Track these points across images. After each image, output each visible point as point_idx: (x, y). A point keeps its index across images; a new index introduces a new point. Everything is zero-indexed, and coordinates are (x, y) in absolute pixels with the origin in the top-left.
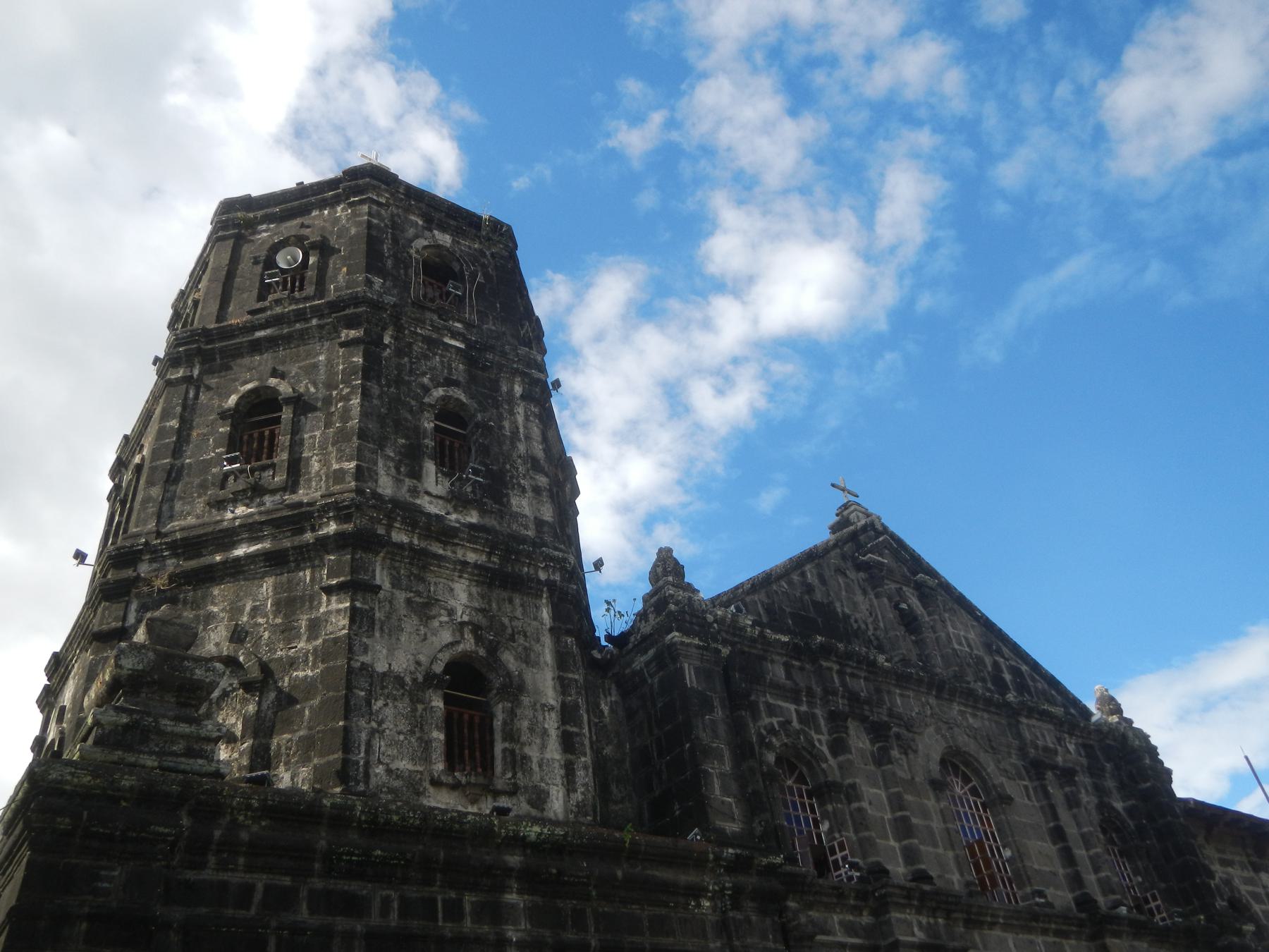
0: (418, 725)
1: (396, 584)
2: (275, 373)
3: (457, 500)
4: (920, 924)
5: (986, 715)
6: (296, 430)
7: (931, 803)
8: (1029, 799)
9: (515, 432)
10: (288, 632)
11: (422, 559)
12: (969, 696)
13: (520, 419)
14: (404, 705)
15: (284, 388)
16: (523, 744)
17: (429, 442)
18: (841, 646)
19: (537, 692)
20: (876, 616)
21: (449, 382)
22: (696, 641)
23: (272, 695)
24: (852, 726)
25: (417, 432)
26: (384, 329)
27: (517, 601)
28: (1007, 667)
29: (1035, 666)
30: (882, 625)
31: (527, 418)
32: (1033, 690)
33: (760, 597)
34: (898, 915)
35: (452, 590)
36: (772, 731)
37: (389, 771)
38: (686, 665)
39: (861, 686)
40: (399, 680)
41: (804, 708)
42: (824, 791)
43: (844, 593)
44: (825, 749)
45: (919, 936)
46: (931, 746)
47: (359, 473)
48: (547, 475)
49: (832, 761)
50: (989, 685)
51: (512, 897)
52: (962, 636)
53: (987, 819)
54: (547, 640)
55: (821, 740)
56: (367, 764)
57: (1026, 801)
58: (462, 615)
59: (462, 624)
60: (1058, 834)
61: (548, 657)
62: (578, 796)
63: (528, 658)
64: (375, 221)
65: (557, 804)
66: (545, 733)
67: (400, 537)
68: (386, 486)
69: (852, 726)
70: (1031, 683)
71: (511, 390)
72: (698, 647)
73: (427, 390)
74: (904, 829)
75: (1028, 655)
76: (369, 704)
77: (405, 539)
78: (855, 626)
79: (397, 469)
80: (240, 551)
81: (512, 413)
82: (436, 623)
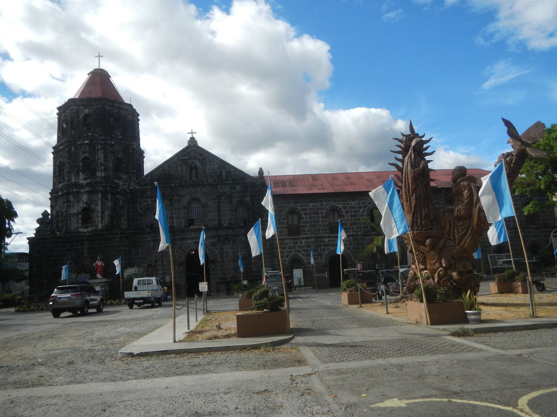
0: (78, 220)
1: (74, 198)
2: (62, 157)
3: (85, 179)
5: (209, 187)
6: (64, 170)
8: (215, 204)
9: (98, 158)
11: (78, 193)
13: (100, 154)
15: (62, 161)
21: (86, 152)
22: (122, 197)
23: (63, 217)
25: (79, 166)
27: (95, 195)
30: (184, 173)
31: (101, 154)
35: (83, 197)
36: (144, 206)
37: (74, 227)
38: (121, 201)
40: (74, 214)
46: (186, 200)
47: (69, 180)
48: (103, 166)
50: (216, 178)
51: (86, 243)
54: (100, 200)
57: (214, 204)
58: (85, 201)
59: (84, 203)
60: (219, 211)
61: (100, 203)
62: (103, 225)
63: (96, 205)
64: (72, 115)
65: (100, 226)
66: (98, 216)
67: (75, 190)
68: (73, 180)
70: (232, 173)
71: (98, 147)
73: (80, 156)
76: (70, 219)
77: (75, 190)
78: (175, 176)
80: (60, 193)
81: (98, 153)
82: (80, 203)
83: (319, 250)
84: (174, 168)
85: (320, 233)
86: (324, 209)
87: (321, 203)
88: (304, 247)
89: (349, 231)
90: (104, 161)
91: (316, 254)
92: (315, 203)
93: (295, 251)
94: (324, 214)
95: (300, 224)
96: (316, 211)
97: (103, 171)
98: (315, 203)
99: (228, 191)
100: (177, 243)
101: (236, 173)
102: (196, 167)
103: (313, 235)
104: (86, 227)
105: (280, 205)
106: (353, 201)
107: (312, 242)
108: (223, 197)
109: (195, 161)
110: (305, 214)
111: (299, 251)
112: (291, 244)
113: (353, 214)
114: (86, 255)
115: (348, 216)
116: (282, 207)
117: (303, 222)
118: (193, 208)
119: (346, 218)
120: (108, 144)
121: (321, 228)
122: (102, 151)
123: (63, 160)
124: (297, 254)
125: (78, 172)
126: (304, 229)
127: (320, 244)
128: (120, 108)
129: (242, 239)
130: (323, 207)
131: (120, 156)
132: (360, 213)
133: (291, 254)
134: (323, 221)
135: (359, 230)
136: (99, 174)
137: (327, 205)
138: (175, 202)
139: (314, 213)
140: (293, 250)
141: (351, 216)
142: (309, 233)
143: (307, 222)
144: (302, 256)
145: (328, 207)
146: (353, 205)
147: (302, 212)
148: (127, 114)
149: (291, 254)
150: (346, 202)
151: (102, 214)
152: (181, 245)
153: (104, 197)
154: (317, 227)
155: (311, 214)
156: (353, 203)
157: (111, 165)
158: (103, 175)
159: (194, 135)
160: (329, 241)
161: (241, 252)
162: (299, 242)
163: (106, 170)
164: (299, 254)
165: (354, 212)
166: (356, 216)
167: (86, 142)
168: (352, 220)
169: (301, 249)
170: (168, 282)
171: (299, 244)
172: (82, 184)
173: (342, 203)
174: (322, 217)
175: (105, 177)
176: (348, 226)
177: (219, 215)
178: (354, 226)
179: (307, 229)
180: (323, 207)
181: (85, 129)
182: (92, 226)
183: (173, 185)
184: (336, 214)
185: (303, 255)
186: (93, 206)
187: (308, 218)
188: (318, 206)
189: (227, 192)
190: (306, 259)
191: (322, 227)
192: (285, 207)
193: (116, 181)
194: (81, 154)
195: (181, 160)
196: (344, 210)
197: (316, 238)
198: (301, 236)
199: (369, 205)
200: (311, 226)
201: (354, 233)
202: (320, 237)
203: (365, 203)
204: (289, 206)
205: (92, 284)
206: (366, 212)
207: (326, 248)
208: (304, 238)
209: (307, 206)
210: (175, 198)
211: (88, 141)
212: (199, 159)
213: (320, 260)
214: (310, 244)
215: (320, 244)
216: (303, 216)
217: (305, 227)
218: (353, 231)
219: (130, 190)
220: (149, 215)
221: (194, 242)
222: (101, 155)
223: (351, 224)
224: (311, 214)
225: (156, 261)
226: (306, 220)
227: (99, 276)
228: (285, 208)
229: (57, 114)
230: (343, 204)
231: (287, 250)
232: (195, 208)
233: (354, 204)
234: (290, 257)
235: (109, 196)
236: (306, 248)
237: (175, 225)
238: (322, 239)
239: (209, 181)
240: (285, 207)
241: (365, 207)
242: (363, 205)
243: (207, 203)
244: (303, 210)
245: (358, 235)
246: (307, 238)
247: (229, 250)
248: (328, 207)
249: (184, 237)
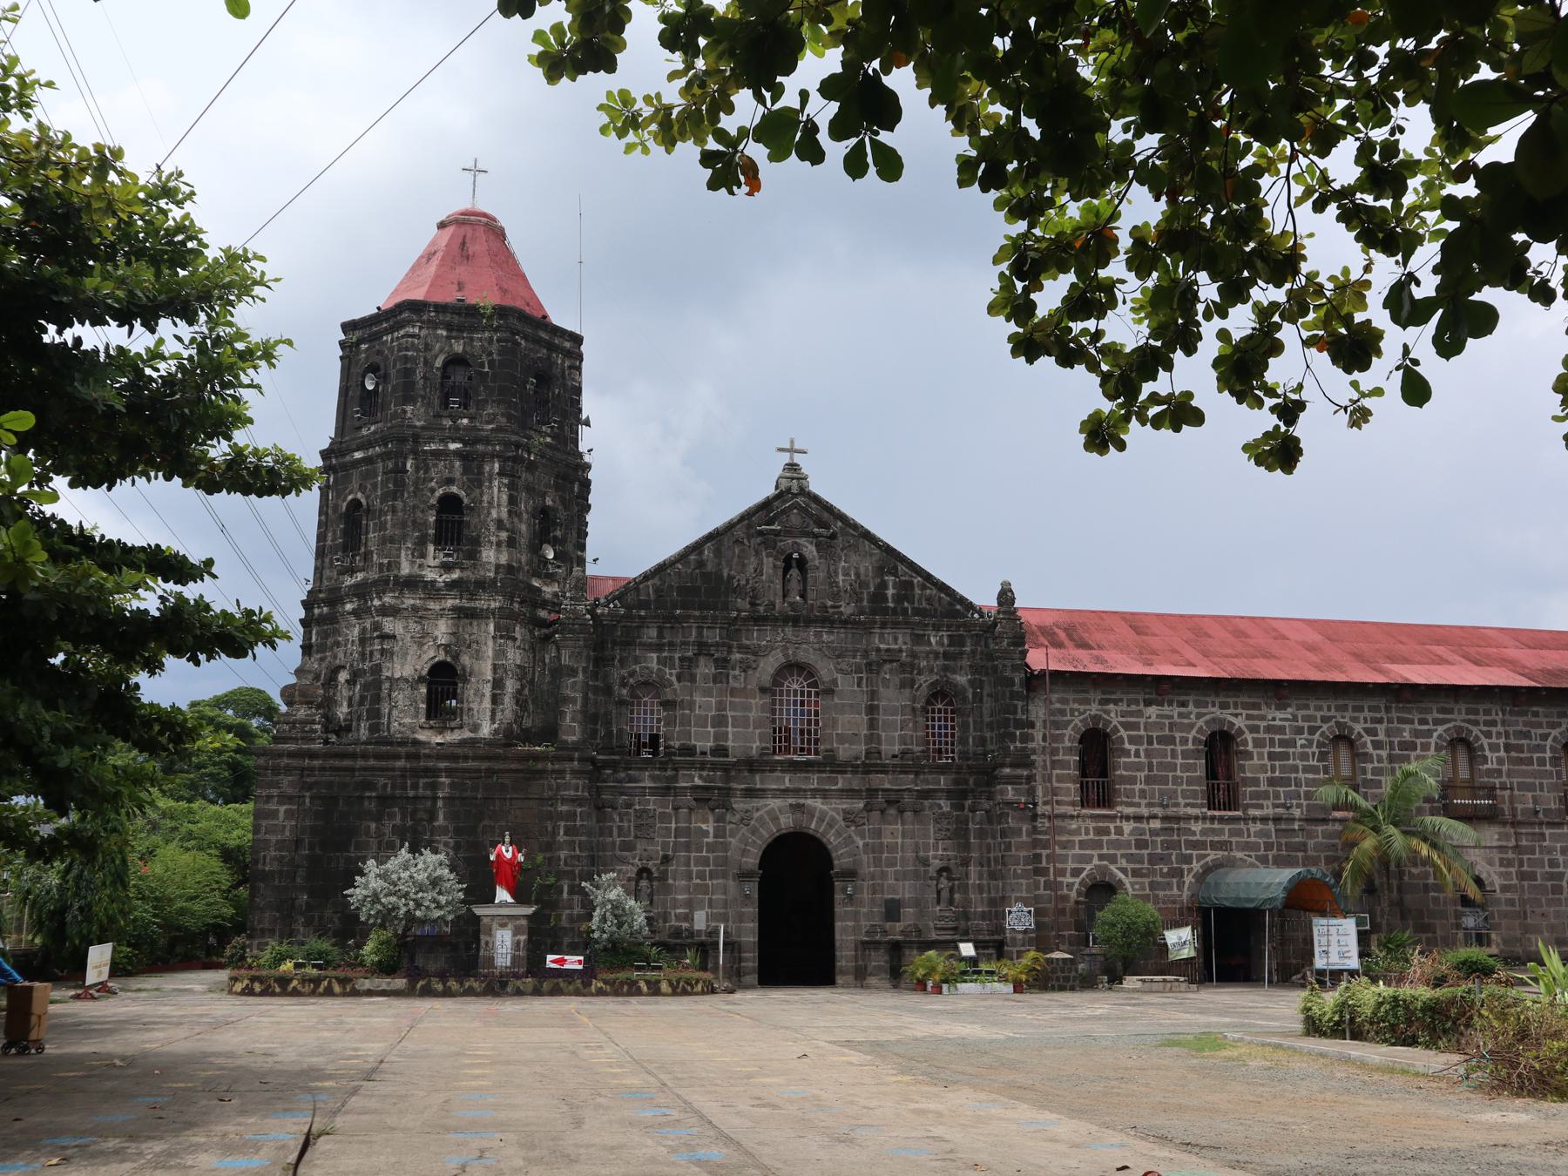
2: (362, 488)
3: (447, 568)
4: (701, 777)
7: (757, 701)
8: (859, 685)
10: (363, 654)
12: (827, 620)
14: (408, 692)
15: (363, 501)
16: (469, 703)
17: (432, 532)
18: (697, 613)
19: (481, 673)
20: (761, 572)
21: (450, 481)
24: (702, 661)
25: (426, 522)
26: (406, 458)
27: (475, 623)
28: (895, 583)
29: (928, 577)
31: (499, 491)
33: (656, 581)
36: (632, 674)
39: (713, 636)
40: (406, 680)
41: (665, 654)
42: (668, 705)
43: (736, 559)
44: (674, 679)
45: (698, 782)
46: (768, 666)
49: (676, 685)
52: (850, 568)
53: (816, 702)
54: (490, 643)
55: (671, 674)
56: (389, 723)
57: (856, 688)
60: (872, 710)
61: (490, 653)
62: (496, 726)
63: (478, 656)
66: (483, 695)
68: (405, 569)
69: (702, 661)
70: (918, 591)
73: (433, 491)
74: (720, 721)
76: (390, 695)
79: (413, 554)
81: (490, 487)
83: (1173, 858)
84: (736, 559)
85: (1176, 805)
86: (1191, 726)
87: (1182, 710)
88: (1128, 845)
89: (1265, 803)
90: (510, 512)
91: (1165, 870)
92: (1166, 707)
93: (1101, 857)
94: (1190, 746)
95: (1118, 773)
96: (1167, 732)
97: (504, 548)
98: (1166, 707)
99: (904, 647)
100: (735, 806)
102: (802, 563)
103: (1158, 811)
104: (441, 730)
105: (1058, 706)
106: (1279, 708)
107: (1153, 832)
108: (887, 667)
109: (802, 541)
110: (1132, 740)
111: (1113, 859)
112: (1087, 833)
113: (1278, 750)
114: (441, 820)
115: (1261, 756)
116: (1062, 712)
117: (1128, 767)
118: (788, 695)
119: (1256, 761)
120: (522, 459)
121: (1179, 788)
122: (506, 481)
123: (367, 498)
124: (1106, 866)
125: (421, 543)
126: (1128, 787)
127: (1175, 837)
128: (552, 347)
129: (941, 808)
130: (1186, 721)
131: (549, 502)
132: (1299, 750)
133: (1088, 867)
134: (1186, 768)
135: (1294, 802)
136: (489, 555)
137: (1199, 716)
138: (733, 669)
139: (1161, 740)
140: (1095, 853)
141: (1272, 756)
142: (1144, 802)
143: (1139, 767)
144: (1121, 875)
145: (1201, 722)
146: (1277, 723)
147: (1123, 733)
148: (570, 367)
149: (1088, 867)
150: (1255, 712)
151: (493, 688)
152: (747, 811)
153: (504, 633)
154: (1170, 786)
155: (1150, 742)
156: (1279, 715)
157: (523, 528)
158: (503, 559)
159: (798, 458)
160: (1204, 832)
162: (1112, 826)
163: (511, 543)
164: (1112, 867)
165: (1283, 743)
166: (1285, 756)
167: (453, 446)
168: (1273, 771)
169: (1119, 853)
170: (699, 931)
171: (1113, 837)
172: (434, 582)
173: (1245, 712)
174: (1185, 754)
175: (510, 568)
176: (1263, 788)
177: (872, 724)
178: (1281, 789)
179: (1137, 787)
180: (1186, 721)
181: (454, 402)
182: (461, 727)
183: (734, 614)
184: (1344, 754)
185: (1124, 871)
186: (466, 660)
187: (1142, 754)
188: (1172, 717)
189: (900, 651)
190: (1132, 884)
191: (1184, 787)
192: (1072, 711)
193: (536, 583)
194: (433, 484)
195: (761, 533)
196: (1249, 737)
197: (1165, 819)
198: (1119, 808)
199: (1325, 727)
200: (1148, 780)
201: (1280, 810)
202: (1178, 819)
203: (1314, 718)
204: (1085, 711)
205: (485, 920)
206: (1314, 749)
207: (1195, 853)
208: (1128, 818)
209: (1139, 714)
210: (737, 656)
211: (458, 445)
212: (816, 536)
213: (1175, 891)
214: (1147, 837)
215: (1175, 837)
216: (1127, 746)
217: (1132, 780)
218: (1276, 806)
219: (594, 616)
220: (645, 703)
221: (791, 805)
222: (496, 494)
223: (1272, 782)
224: (1150, 742)
225: (666, 860)
226: (1137, 760)
227: (502, 895)
228: (1072, 715)
229: (342, 344)
230: (1249, 717)
231: (1077, 851)
232: (795, 695)
233: (1281, 720)
234: (1083, 875)
235: (519, 632)
236: (1134, 851)
237: (730, 744)
238: (1182, 825)
239: (842, 609)
240: (1072, 711)
241: (1312, 730)
242: (1306, 725)
243: (835, 681)
244: (1127, 726)
245: (1294, 819)
246: (1138, 818)
247: (900, 841)
248: (1201, 722)
249: (758, 786)
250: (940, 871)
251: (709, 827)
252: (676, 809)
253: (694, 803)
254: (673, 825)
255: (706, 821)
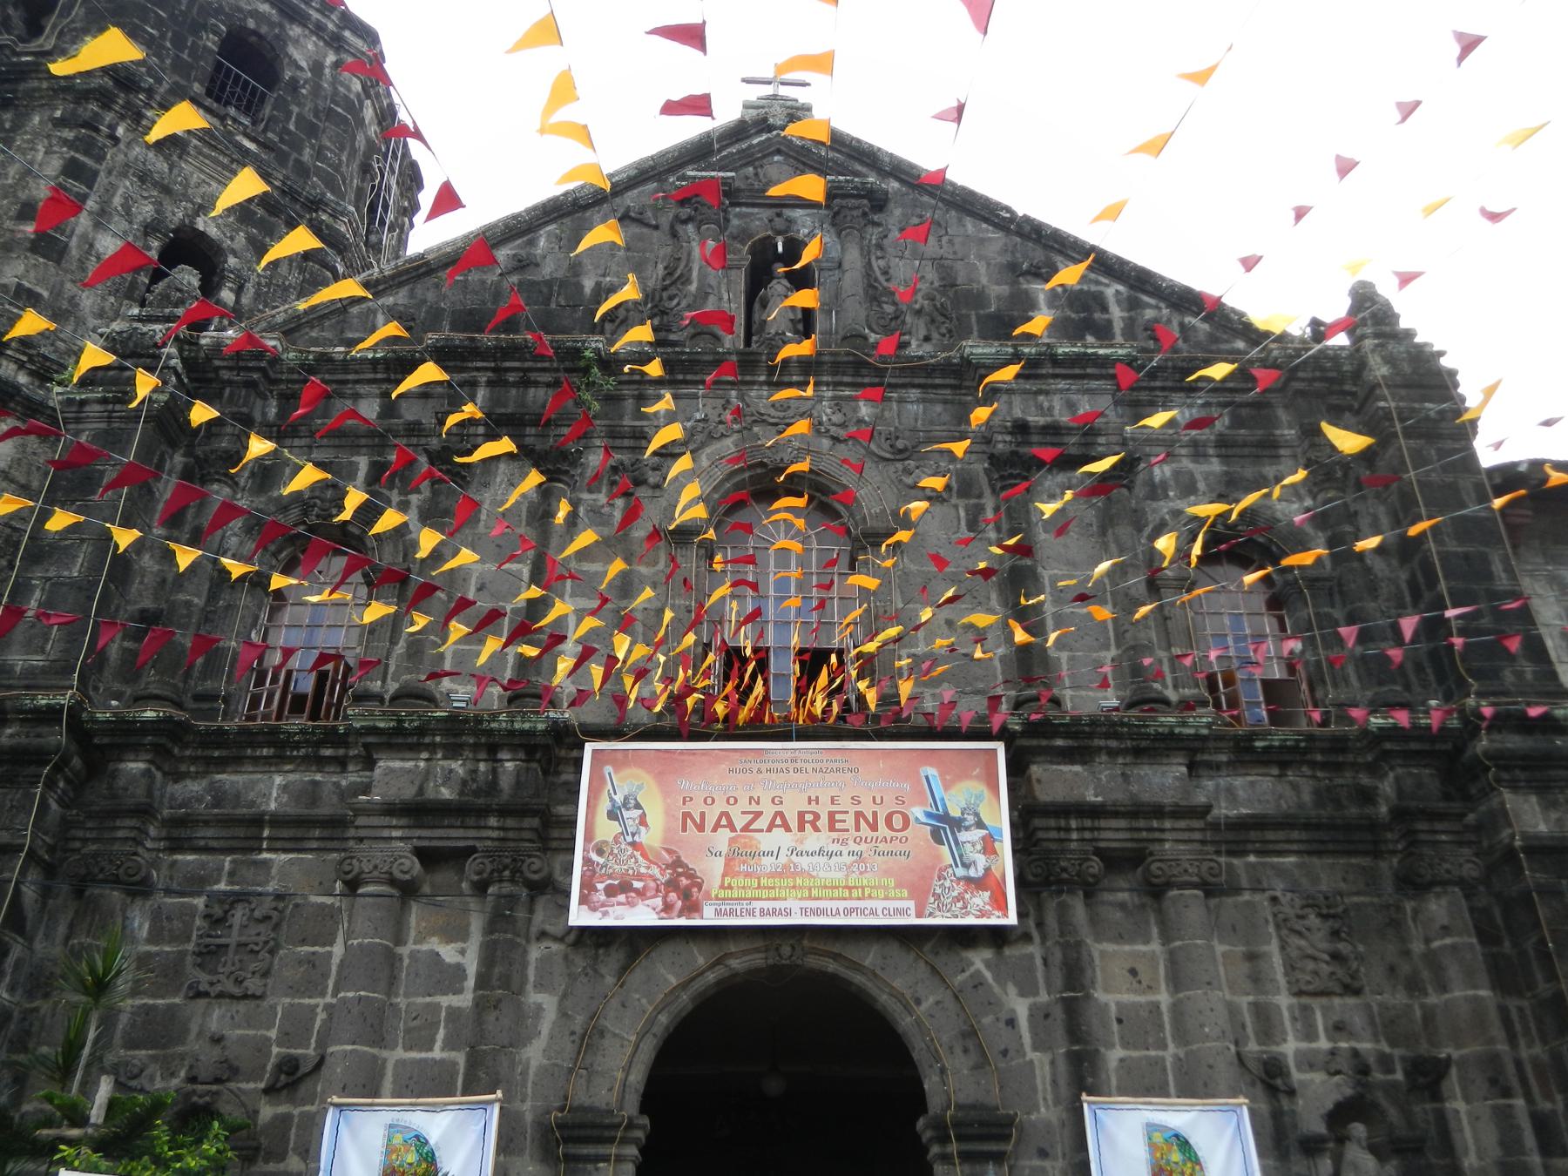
5: (914, 394)
32: (1118, 326)
34: (397, 764)
72: (104, 401)
75: (1122, 262)
101: (1149, 314)
122: (69, 134)
148: (337, 65)
161: (1310, 1035)
250: (1340, 1116)
251: (465, 955)
252: (352, 886)
253: (415, 866)
254: (338, 950)
255: (456, 934)
